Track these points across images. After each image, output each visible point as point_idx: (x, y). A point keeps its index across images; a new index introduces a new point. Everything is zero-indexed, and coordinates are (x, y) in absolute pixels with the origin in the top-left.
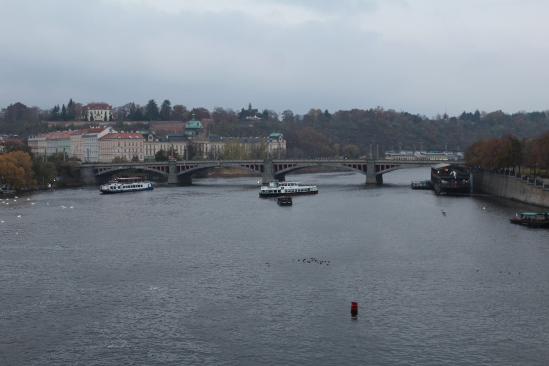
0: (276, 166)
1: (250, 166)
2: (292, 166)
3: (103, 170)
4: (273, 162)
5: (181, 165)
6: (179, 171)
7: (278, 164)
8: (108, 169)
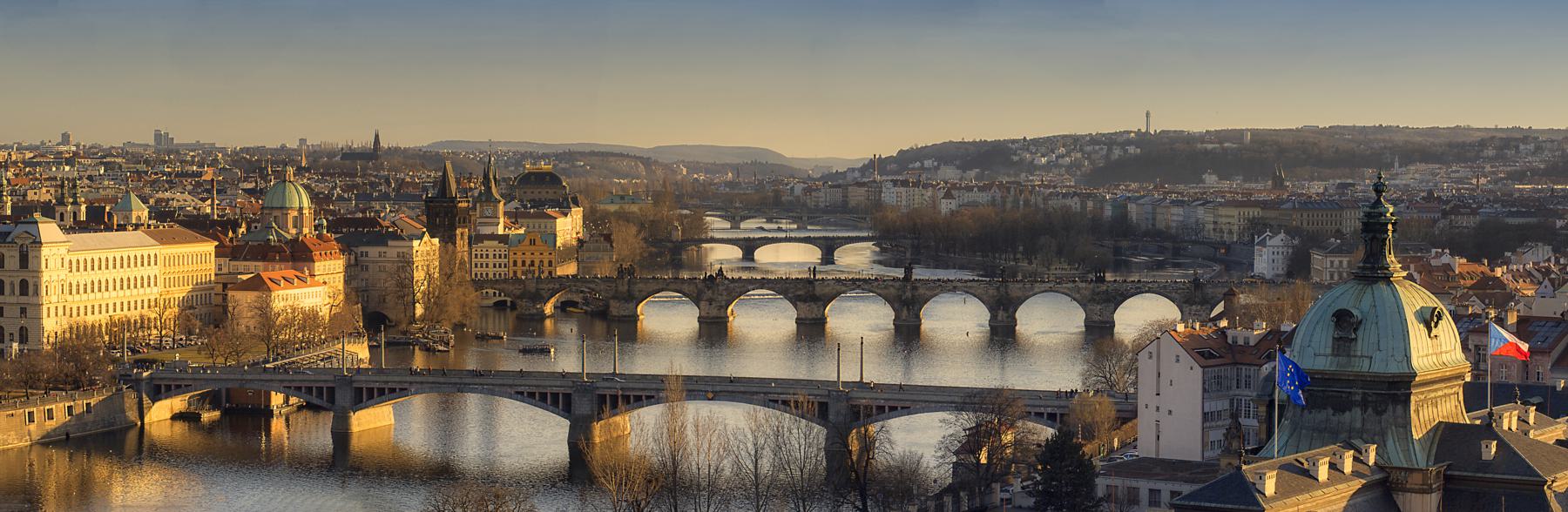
1: (537, 395)
3: (173, 387)
8: (186, 386)
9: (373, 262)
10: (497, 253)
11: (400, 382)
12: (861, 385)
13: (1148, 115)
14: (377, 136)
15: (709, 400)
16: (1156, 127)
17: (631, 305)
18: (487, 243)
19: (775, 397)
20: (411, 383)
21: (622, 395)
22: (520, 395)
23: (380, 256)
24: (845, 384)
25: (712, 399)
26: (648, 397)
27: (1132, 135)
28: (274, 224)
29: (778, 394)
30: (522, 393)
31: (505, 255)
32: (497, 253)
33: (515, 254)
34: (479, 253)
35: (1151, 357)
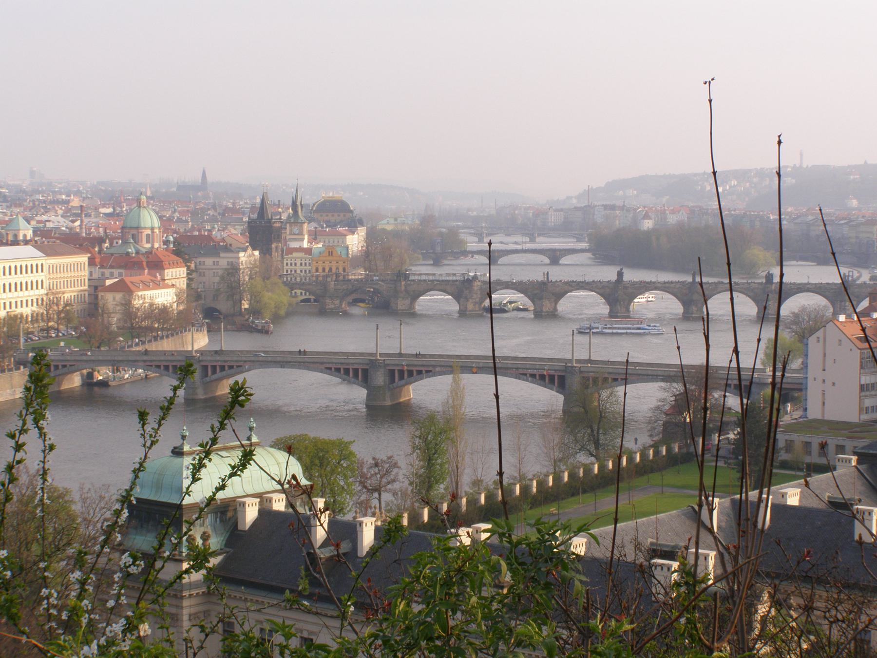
0: (392, 372)
1: (342, 370)
2: (424, 372)
3: (60, 367)
4: (388, 365)
5: (209, 364)
6: (206, 376)
7: (396, 368)
8: (71, 365)
9: (209, 269)
11: (236, 361)
12: (590, 361)
13: (801, 155)
14: (204, 173)
15: (473, 373)
16: (808, 163)
17: (407, 302)
18: (295, 255)
19: (525, 371)
20: (245, 361)
21: (408, 371)
22: (328, 370)
23: (214, 264)
24: (578, 361)
25: (476, 373)
26: (427, 372)
27: (789, 169)
28: (132, 241)
29: (527, 369)
30: (330, 369)
31: (310, 265)
34: (289, 262)
35: (818, 341)
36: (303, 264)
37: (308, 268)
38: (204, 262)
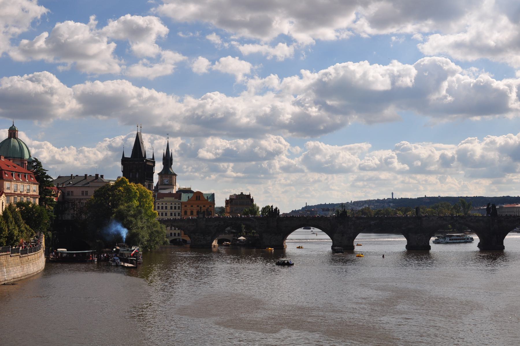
10: (173, 206)
18: (166, 199)
23: (83, 194)
31: (179, 207)
32: (173, 206)
33: (186, 206)
34: (160, 206)
36: (173, 208)
37: (177, 211)
38: (72, 192)
